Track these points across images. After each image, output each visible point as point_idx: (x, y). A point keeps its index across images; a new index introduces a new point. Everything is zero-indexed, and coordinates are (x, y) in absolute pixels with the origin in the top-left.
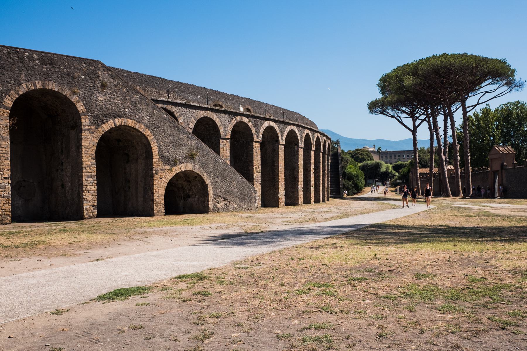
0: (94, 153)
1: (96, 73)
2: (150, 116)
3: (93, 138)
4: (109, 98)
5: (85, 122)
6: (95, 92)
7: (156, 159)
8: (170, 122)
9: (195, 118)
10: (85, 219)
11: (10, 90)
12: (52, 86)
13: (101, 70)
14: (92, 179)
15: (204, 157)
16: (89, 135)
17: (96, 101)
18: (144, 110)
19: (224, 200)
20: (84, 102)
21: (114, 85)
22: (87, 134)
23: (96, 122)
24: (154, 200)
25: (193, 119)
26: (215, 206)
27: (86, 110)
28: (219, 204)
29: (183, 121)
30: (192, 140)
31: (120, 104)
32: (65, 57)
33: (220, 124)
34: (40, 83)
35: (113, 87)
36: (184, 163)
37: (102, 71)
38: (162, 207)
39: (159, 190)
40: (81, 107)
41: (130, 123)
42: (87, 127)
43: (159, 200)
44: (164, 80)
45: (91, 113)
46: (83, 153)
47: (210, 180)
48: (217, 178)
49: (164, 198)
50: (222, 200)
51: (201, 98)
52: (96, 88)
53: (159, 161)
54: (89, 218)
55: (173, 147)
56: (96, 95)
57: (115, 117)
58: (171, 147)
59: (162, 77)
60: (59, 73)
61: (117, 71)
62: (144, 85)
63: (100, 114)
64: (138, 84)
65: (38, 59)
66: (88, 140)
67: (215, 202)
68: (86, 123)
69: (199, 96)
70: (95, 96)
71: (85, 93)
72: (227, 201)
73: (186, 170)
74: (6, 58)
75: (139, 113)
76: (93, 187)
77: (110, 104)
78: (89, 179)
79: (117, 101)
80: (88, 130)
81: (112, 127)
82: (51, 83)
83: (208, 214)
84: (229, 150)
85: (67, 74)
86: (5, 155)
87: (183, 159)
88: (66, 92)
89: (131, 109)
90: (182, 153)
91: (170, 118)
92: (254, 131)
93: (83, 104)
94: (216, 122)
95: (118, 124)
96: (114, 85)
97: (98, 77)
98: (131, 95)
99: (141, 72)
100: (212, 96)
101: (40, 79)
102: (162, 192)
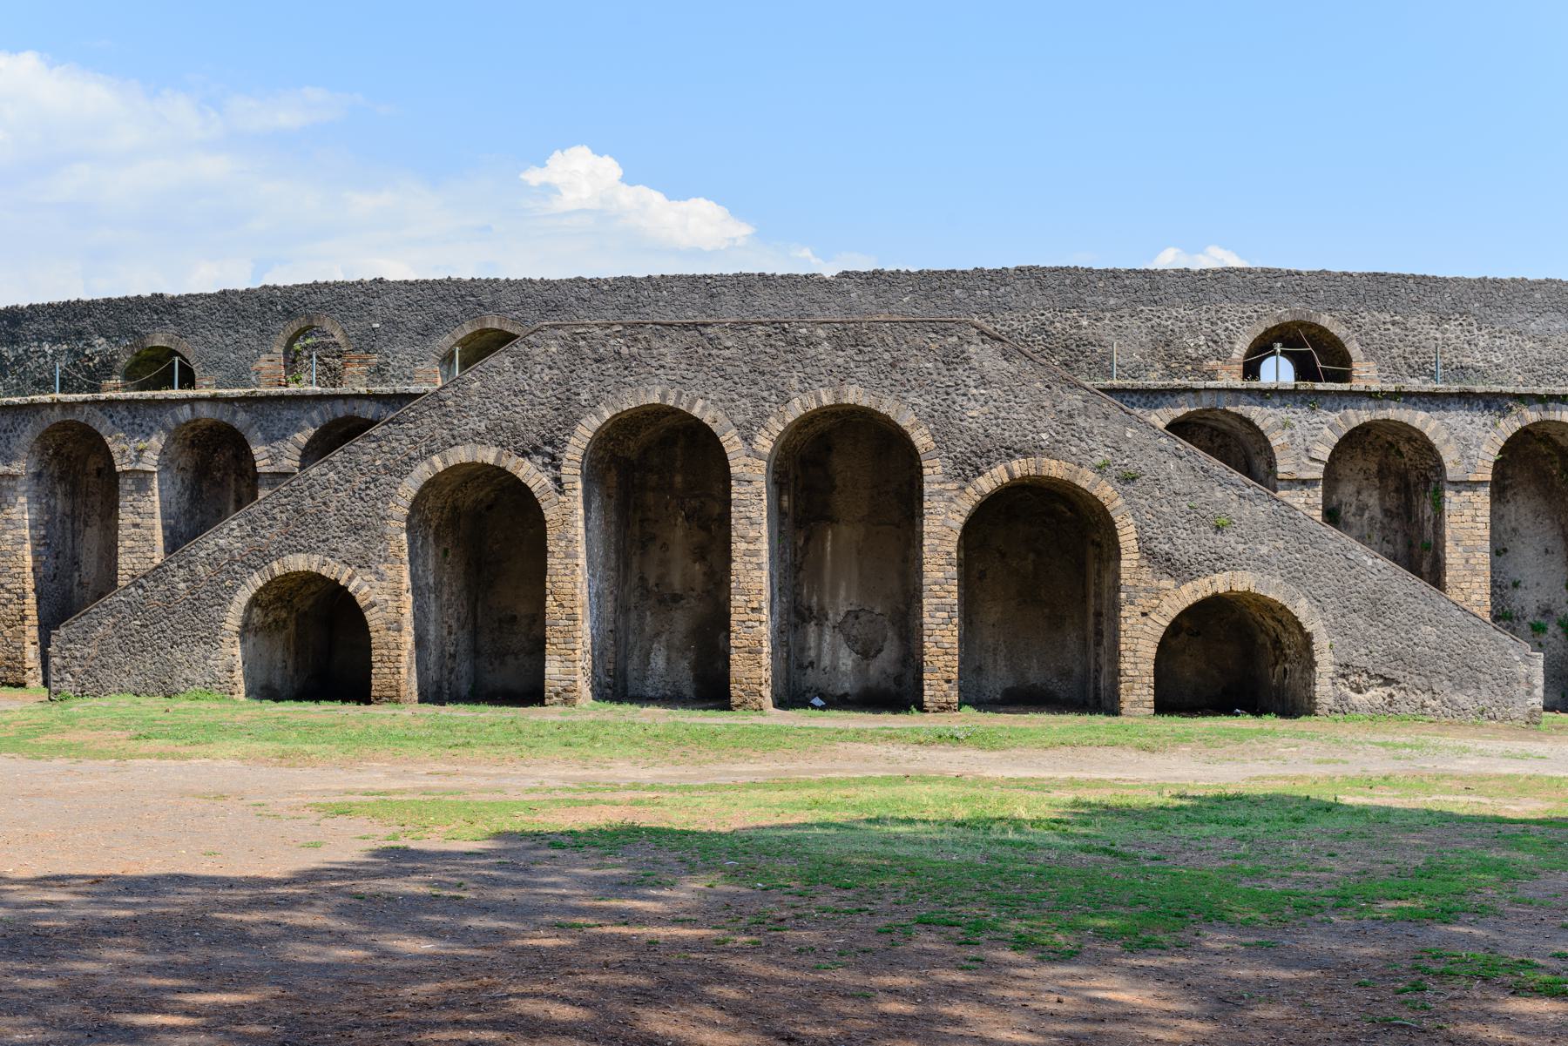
0: (952, 548)
1: (963, 352)
2: (1115, 445)
3: (952, 512)
4: (994, 410)
5: (934, 472)
6: (959, 399)
7: (1130, 559)
8: (1181, 458)
9: (1331, 427)
10: (927, 711)
11: (768, 416)
12: (854, 395)
13: (976, 340)
15: (1299, 551)
16: (941, 506)
17: (961, 420)
18: (1096, 432)
19: (1380, 681)
20: (932, 426)
21: (1009, 375)
22: (936, 504)
23: (960, 471)
24: (1122, 673)
25: (1326, 431)
26: (1342, 699)
27: (934, 445)
28: (1360, 692)
29: (1286, 440)
30: (1257, 502)
31: (1024, 423)
32: (887, 325)
33: (1445, 436)
34: (830, 393)
35: (1006, 380)
36: (1225, 570)
37: (977, 345)
38: (1145, 692)
39: (1139, 646)
41: (1054, 469)
42: (937, 487)
43: (1137, 673)
44: (1421, 280)
45: (948, 452)
47: (1323, 619)
48: (1354, 615)
49: (1153, 667)
50: (1373, 682)
52: (962, 386)
54: (936, 709)
55: (1187, 526)
56: (961, 406)
57: (1011, 457)
58: (1180, 525)
59: (1417, 273)
60: (873, 364)
61: (1252, 276)
62: (1345, 307)
63: (972, 452)
64: (1326, 306)
65: (828, 339)
66: (939, 517)
67: (1342, 688)
68: (933, 477)
70: (959, 408)
71: (933, 404)
72: (1394, 685)
73: (1231, 591)
74: (762, 347)
75: (1081, 440)
76: (950, 633)
77: (998, 425)
78: (938, 614)
79: (1015, 416)
80: (940, 493)
81: (1002, 483)
83: (1313, 718)
84: (1487, 520)
85: (891, 365)
86: (754, 560)
87: (1222, 558)
88: (888, 407)
89: (1058, 433)
90: (1218, 542)
91: (1179, 446)
93: (927, 432)
94: (1427, 432)
95: (1018, 474)
96: (1009, 375)
97: (967, 359)
98: (1058, 396)
99: (1336, 268)
101: (831, 384)
102: (1149, 650)
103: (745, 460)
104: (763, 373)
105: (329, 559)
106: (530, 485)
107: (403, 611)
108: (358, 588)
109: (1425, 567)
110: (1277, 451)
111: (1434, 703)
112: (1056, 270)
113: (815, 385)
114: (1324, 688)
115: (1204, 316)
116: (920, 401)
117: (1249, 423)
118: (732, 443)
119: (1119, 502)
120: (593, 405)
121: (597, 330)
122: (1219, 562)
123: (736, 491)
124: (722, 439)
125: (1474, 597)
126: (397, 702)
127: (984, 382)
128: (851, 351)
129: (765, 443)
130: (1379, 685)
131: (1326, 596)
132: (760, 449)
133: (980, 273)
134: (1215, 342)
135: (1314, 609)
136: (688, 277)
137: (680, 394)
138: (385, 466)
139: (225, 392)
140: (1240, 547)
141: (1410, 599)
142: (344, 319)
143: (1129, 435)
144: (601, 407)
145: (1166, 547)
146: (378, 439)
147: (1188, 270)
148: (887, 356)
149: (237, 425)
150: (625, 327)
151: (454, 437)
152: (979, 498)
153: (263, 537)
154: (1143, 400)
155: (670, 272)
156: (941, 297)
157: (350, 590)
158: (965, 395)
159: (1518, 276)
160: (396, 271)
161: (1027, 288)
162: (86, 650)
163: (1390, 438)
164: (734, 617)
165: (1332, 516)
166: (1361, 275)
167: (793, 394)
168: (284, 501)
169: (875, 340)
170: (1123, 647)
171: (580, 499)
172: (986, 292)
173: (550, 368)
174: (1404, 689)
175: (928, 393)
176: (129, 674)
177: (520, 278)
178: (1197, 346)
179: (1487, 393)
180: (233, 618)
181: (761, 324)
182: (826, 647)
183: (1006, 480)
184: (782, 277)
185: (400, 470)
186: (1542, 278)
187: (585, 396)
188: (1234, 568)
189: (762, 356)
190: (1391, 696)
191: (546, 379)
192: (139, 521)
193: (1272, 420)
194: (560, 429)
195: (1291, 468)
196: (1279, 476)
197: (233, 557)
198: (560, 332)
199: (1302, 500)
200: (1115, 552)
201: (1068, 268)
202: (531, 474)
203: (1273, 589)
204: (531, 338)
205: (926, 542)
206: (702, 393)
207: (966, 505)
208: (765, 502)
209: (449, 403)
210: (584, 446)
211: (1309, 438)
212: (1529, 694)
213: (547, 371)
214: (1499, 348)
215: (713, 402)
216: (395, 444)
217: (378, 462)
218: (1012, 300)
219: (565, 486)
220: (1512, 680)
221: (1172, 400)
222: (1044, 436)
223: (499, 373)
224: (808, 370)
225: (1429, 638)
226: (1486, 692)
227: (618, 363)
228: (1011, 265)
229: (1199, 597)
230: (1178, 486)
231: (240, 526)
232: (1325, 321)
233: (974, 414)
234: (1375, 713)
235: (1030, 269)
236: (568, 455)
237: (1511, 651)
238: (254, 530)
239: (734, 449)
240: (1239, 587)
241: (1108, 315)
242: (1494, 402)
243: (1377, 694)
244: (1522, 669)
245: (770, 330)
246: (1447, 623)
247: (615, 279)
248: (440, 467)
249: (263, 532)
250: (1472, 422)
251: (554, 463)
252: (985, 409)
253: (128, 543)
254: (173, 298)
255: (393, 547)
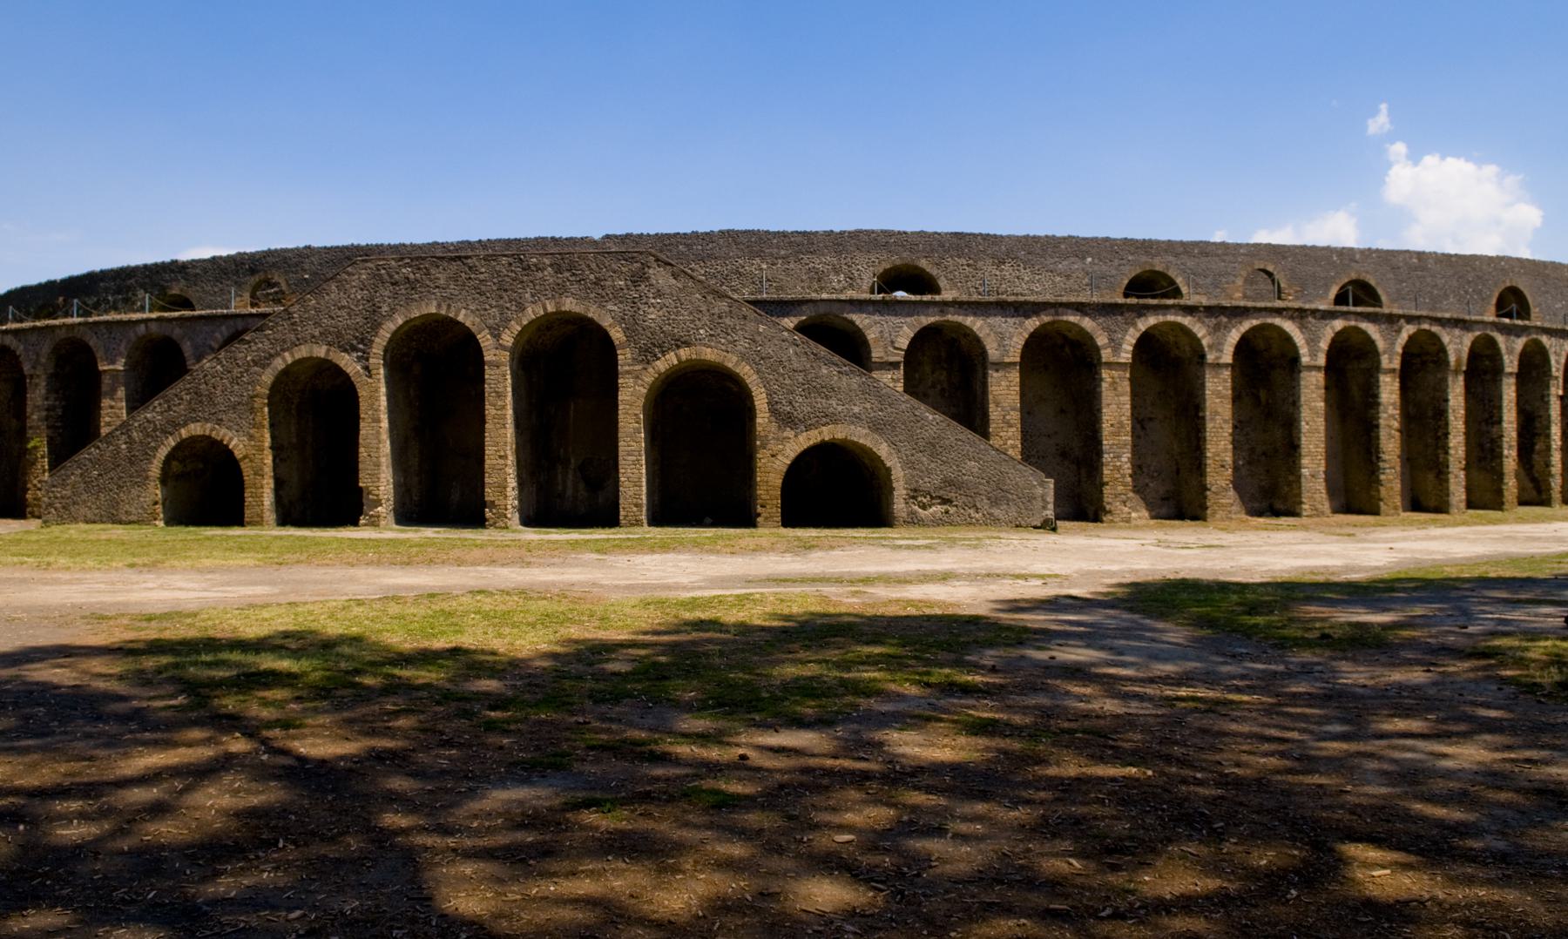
5: (624, 357)
6: (642, 306)
7: (762, 418)
12: (570, 305)
13: (655, 265)
14: (635, 458)
15: (881, 410)
26: (913, 513)
27: (625, 338)
34: (553, 304)
35: (674, 292)
40: (617, 335)
41: (710, 354)
44: (986, 237)
46: (620, 412)
50: (934, 501)
51: (1096, 261)
53: (770, 422)
57: (678, 347)
59: (983, 232)
65: (551, 265)
69: (1089, 259)
77: (669, 324)
82: (568, 300)
88: (593, 312)
89: (711, 329)
92: (1101, 340)
94: (975, 329)
95: (684, 358)
97: (648, 279)
100: (1132, 254)
102: (777, 481)
103: (493, 352)
104: (506, 290)
105: (217, 426)
106: (348, 371)
107: (266, 461)
108: (236, 445)
109: (978, 422)
110: (871, 342)
111: (977, 516)
112: (745, 232)
113: (543, 298)
114: (899, 506)
115: (843, 261)
116: (615, 308)
117: (852, 323)
118: (485, 340)
119: (755, 377)
120: (390, 316)
121: (393, 263)
122: (833, 419)
123: (489, 373)
124: (478, 337)
125: (1010, 442)
126: (262, 525)
127: (659, 294)
128: (567, 274)
129: (508, 339)
130: (940, 504)
131: (900, 441)
132: (505, 343)
133: (695, 235)
134: (851, 279)
135: (893, 451)
136: (505, 240)
137: (449, 306)
138: (253, 360)
139: (166, 314)
140: (840, 408)
141: (959, 443)
142: (286, 272)
143: (761, 330)
144: (396, 316)
145: (788, 409)
146: (249, 342)
147: (832, 231)
148: (592, 277)
149: (175, 337)
150: (412, 260)
151: (298, 339)
152: (657, 375)
153: (175, 412)
154: (779, 309)
155: (493, 237)
156: (670, 251)
157: (231, 447)
158: (646, 303)
159: (1050, 234)
160: (318, 242)
161: (726, 244)
162: (64, 492)
163: (954, 335)
164: (488, 462)
165: (911, 388)
166: (946, 234)
167: (527, 304)
168: (188, 386)
169: (583, 266)
170: (758, 479)
171: (383, 381)
172: (700, 247)
173: (362, 290)
174: (956, 506)
175: (621, 302)
176: (90, 508)
177: (397, 243)
178: (839, 281)
179: (1015, 302)
180: (155, 469)
181: (505, 256)
182: (569, 484)
183: (676, 362)
184: (566, 239)
185: (263, 362)
186: (1066, 235)
187: (385, 308)
188: (835, 422)
189: (506, 278)
190: (947, 512)
191: (359, 297)
192: (113, 403)
193: (867, 321)
194: (368, 332)
195: (882, 354)
196: (873, 360)
197: (155, 425)
198: (369, 265)
199: (890, 376)
200: (749, 411)
201: (753, 230)
202: (349, 363)
203: (860, 435)
204: (349, 269)
205: (620, 407)
206: (464, 305)
207: (649, 378)
208: (509, 381)
209: (295, 315)
210: (385, 344)
211: (893, 334)
212: (1044, 508)
213: (360, 292)
214: (1038, 281)
215: (472, 311)
216: (260, 345)
217: (249, 358)
218: (717, 252)
219: (374, 372)
220: (1031, 498)
221: (798, 309)
222: (702, 331)
223: (328, 294)
224: (537, 287)
225: (973, 470)
226: (1014, 509)
227: (408, 285)
228: (716, 229)
229: (811, 443)
230: (796, 365)
231: (160, 404)
232: (923, 263)
233: (653, 316)
234: (937, 523)
235: (728, 231)
236: (374, 350)
237: (1031, 478)
238: (169, 407)
239: (486, 344)
240: (840, 436)
241: (780, 261)
242: (1022, 309)
243: (937, 509)
244: (1039, 491)
245: (511, 260)
246: (986, 459)
247: (458, 242)
248: (290, 360)
249: (174, 408)
250: (1006, 322)
251: (364, 358)
252: (661, 313)
253: (107, 419)
254: (183, 263)
255: (258, 419)
